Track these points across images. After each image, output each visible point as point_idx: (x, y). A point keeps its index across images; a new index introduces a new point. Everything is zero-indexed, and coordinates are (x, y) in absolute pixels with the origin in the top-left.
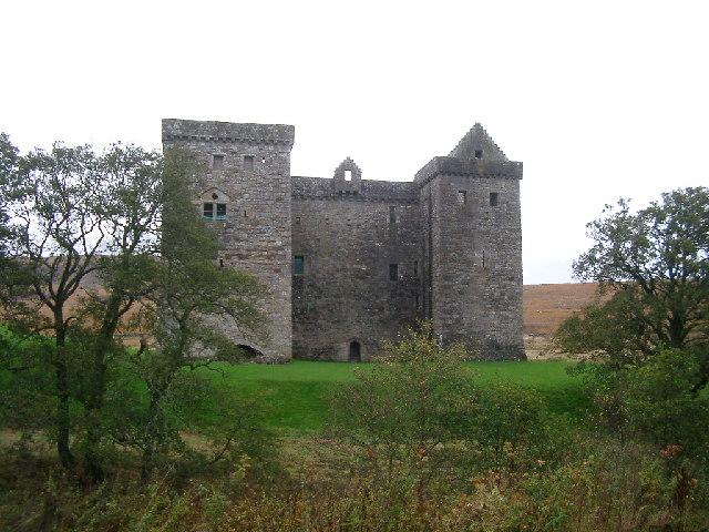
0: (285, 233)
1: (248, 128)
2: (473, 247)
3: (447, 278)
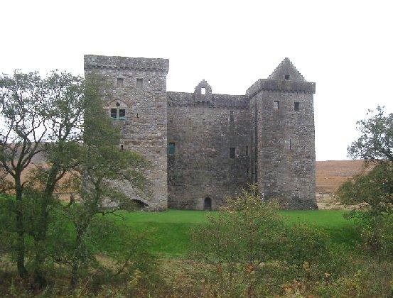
1: (139, 60)
2: (284, 137)
3: (267, 157)
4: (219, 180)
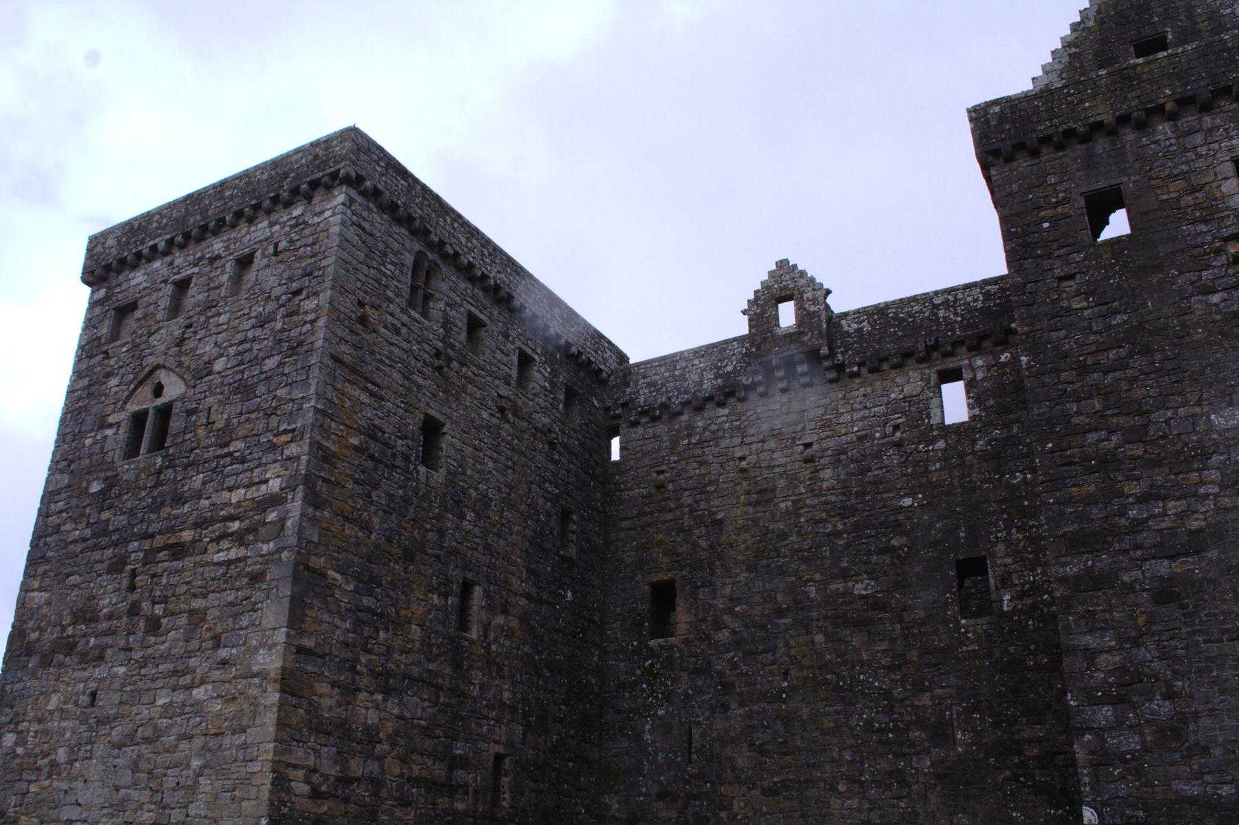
0: (293, 449)
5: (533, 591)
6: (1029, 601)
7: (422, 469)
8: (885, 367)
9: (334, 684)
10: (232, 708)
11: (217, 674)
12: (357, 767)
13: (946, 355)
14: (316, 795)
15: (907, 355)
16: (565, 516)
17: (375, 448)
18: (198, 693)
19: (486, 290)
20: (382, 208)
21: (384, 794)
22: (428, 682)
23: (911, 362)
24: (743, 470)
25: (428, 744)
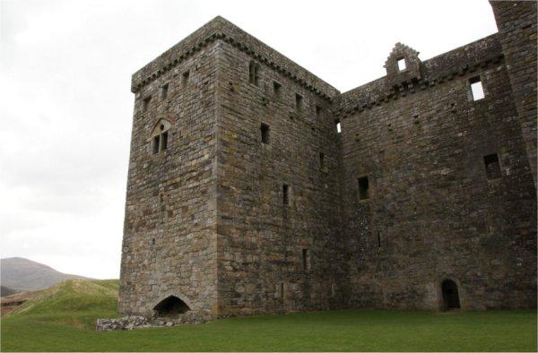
0: (211, 143)
4: (468, 235)
5: (312, 186)
6: (518, 170)
7: (263, 144)
8: (446, 80)
9: (237, 229)
10: (201, 241)
11: (194, 229)
12: (249, 258)
13: (472, 72)
14: (235, 270)
15: (455, 74)
16: (322, 156)
17: (244, 138)
18: (189, 236)
19: (280, 72)
20: (234, 46)
21: (261, 267)
22: (274, 225)
23: (457, 77)
24: (390, 130)
25: (277, 248)
